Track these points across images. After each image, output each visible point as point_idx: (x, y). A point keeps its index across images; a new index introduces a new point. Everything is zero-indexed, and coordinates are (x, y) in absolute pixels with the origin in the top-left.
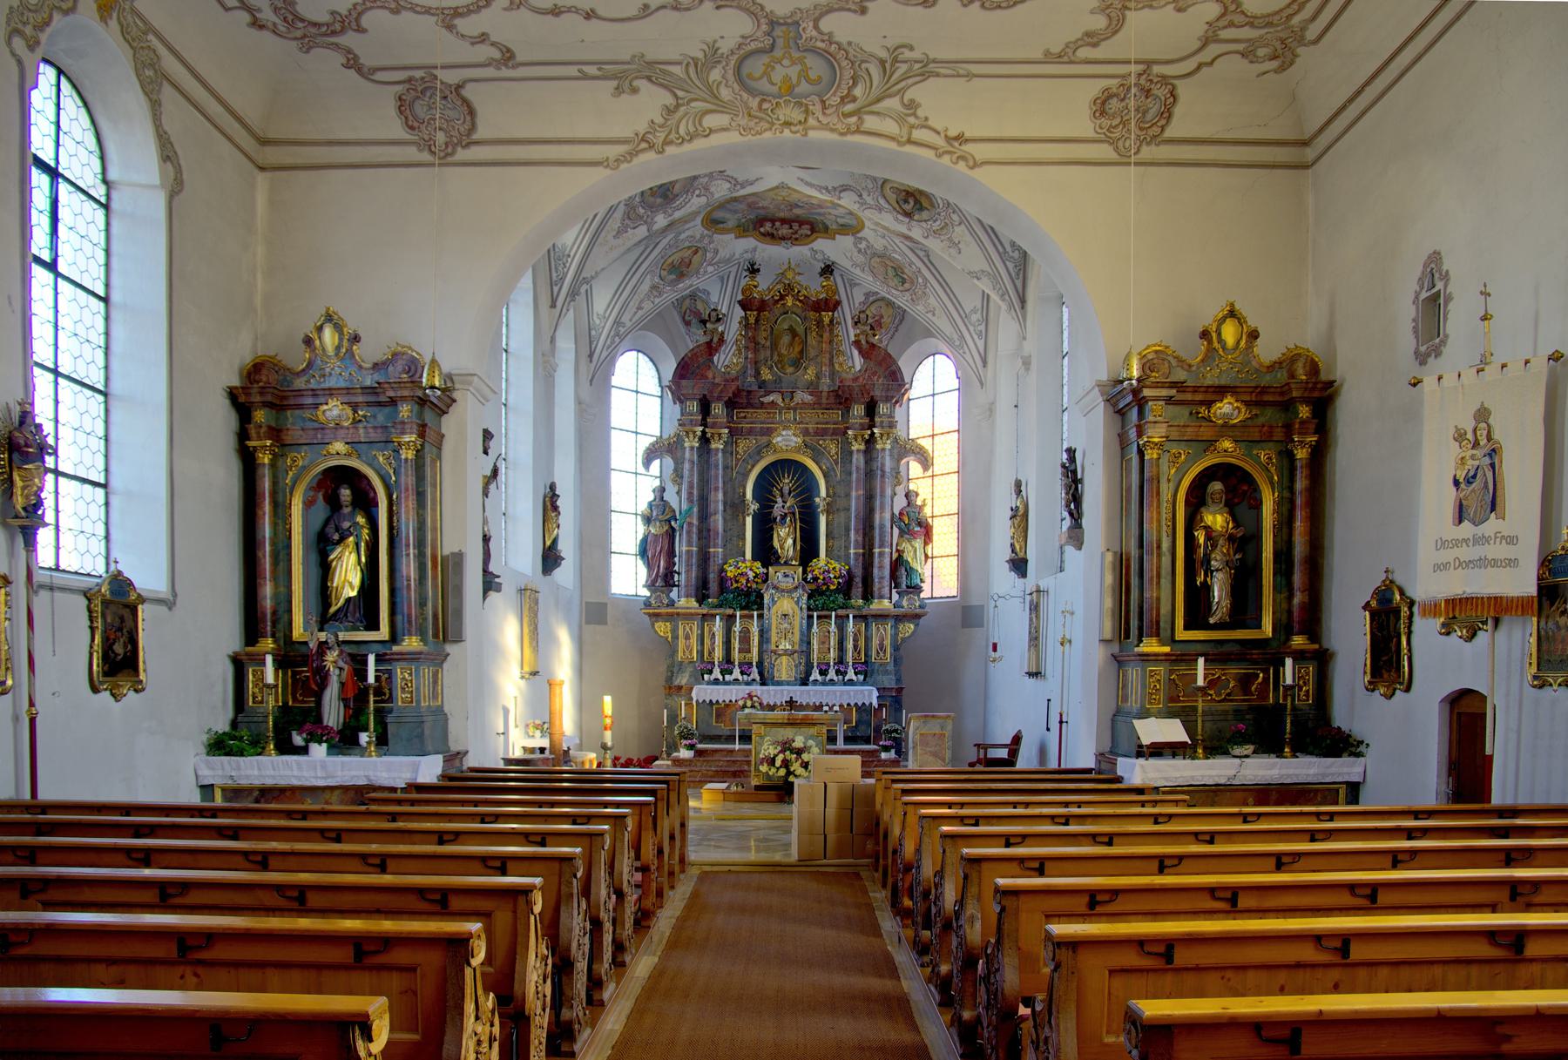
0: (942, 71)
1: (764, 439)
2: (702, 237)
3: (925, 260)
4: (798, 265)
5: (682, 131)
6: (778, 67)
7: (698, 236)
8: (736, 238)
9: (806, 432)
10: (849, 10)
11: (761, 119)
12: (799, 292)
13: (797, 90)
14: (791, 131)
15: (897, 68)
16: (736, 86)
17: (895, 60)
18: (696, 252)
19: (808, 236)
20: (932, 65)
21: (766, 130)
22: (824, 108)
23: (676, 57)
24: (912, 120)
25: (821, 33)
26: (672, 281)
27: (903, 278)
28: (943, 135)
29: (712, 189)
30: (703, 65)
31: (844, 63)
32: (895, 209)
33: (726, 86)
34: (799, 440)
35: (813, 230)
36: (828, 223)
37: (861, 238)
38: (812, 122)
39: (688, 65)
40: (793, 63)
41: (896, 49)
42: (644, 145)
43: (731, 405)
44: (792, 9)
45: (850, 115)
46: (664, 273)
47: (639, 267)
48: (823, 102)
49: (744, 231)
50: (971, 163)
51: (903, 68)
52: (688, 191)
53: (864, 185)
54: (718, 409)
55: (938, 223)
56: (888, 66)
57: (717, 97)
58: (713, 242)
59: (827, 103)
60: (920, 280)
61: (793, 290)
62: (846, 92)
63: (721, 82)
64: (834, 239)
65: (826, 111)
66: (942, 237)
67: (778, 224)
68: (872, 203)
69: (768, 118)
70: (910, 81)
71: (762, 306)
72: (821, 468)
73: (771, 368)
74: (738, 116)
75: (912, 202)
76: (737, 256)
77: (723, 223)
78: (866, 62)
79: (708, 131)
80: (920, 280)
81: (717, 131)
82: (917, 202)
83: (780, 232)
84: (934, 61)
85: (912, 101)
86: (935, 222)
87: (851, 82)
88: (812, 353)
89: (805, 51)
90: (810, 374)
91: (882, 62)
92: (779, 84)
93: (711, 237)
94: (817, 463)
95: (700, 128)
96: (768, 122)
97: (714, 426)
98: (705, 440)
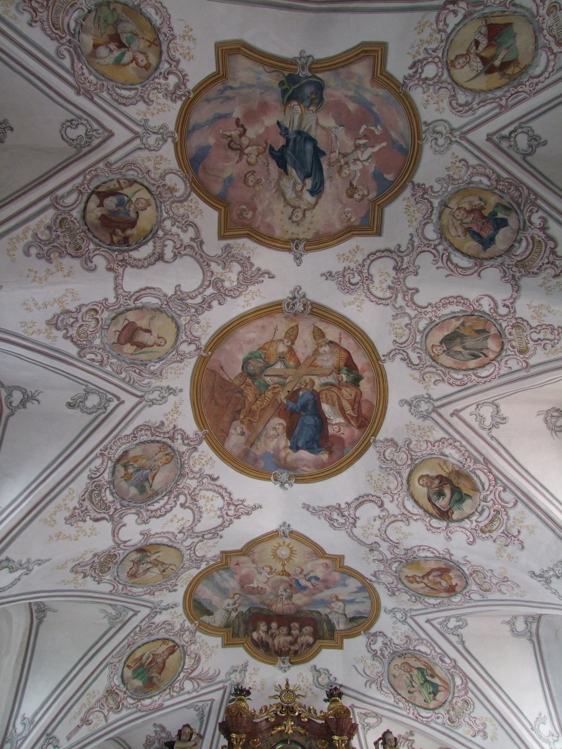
2: (183, 629)
3: (460, 647)
7: (178, 627)
8: (226, 645)
12: (300, 714)
18: (172, 651)
19: (309, 646)
26: (136, 690)
27: (435, 686)
29: (202, 502)
32: (426, 511)
35: (316, 636)
36: (334, 618)
37: (375, 635)
46: (128, 673)
52: (171, 492)
53: (385, 486)
55: (486, 513)
58: (194, 642)
60: (458, 681)
61: (293, 710)
64: (341, 647)
66: (494, 535)
67: (274, 625)
68: (397, 512)
75: (447, 491)
76: (222, 677)
80: (458, 681)
82: (455, 490)
83: (276, 641)
86: (481, 514)
93: (193, 633)
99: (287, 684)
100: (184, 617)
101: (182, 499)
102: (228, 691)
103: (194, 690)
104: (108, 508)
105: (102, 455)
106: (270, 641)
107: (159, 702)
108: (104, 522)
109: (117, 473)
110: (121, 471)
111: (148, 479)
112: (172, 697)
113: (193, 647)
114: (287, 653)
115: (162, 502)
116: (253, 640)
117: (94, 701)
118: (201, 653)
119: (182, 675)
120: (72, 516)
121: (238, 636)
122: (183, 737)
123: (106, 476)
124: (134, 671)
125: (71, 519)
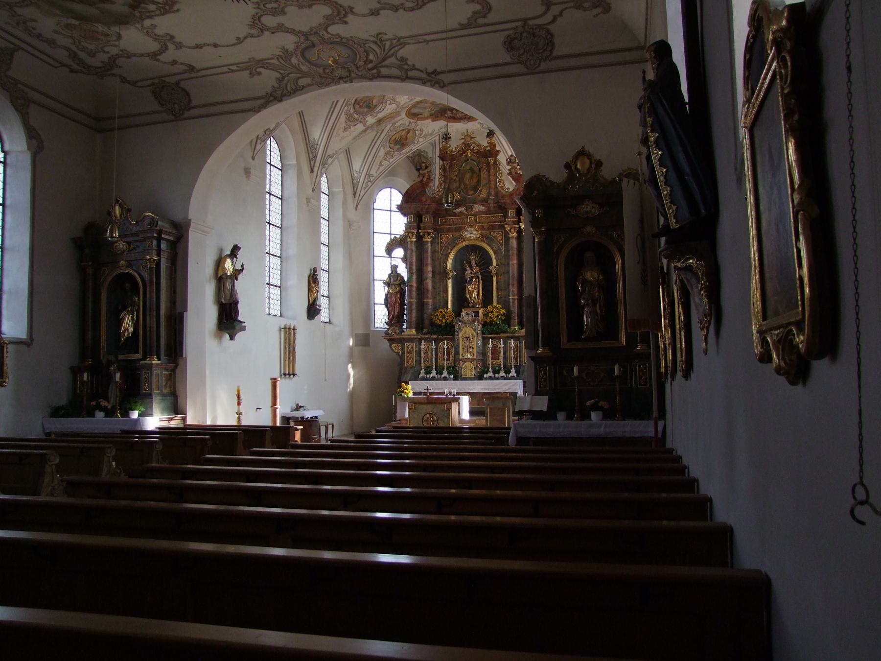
0: (409, 41)
1: (457, 234)
2: (410, 123)
4: (473, 133)
5: (289, 89)
9: (482, 228)
11: (327, 78)
12: (473, 148)
14: (344, 82)
15: (385, 44)
18: (409, 132)
20: (402, 40)
21: (331, 83)
22: (357, 68)
24: (406, 67)
26: (398, 149)
28: (425, 72)
30: (285, 57)
31: (356, 46)
34: (479, 233)
38: (353, 75)
42: (272, 98)
43: (436, 214)
45: (372, 69)
46: (392, 145)
47: (374, 145)
48: (356, 65)
49: (436, 118)
50: (442, 85)
51: (388, 44)
52: (382, 103)
54: (426, 218)
56: (379, 43)
57: (300, 71)
58: (418, 125)
59: (358, 65)
62: (365, 59)
65: (359, 69)
69: (330, 77)
70: (396, 48)
71: (453, 158)
72: (492, 249)
73: (459, 193)
74: (315, 78)
76: (436, 131)
77: (421, 114)
78: (366, 44)
79: (302, 87)
81: (306, 87)
83: (458, 116)
84: (402, 37)
85: (402, 58)
87: (365, 54)
88: (484, 182)
90: (484, 194)
93: (416, 122)
94: (490, 246)
95: (298, 86)
96: (331, 78)
97: (425, 228)
98: (420, 238)
99: (467, 132)
100: (409, 119)
101: (388, 102)
102: (441, 135)
103: (424, 140)
104: (357, 120)
105: (346, 105)
106: (455, 116)
107: (410, 148)
108: (358, 124)
109: (356, 108)
110: (357, 106)
111: (370, 104)
112: (415, 146)
113: (418, 127)
114: (465, 118)
115: (380, 107)
116: (446, 117)
117: (381, 159)
118: (423, 128)
119: (416, 138)
120: (345, 129)
121: (438, 117)
122: (423, 168)
123: (352, 110)
124: (394, 144)
125: (345, 130)
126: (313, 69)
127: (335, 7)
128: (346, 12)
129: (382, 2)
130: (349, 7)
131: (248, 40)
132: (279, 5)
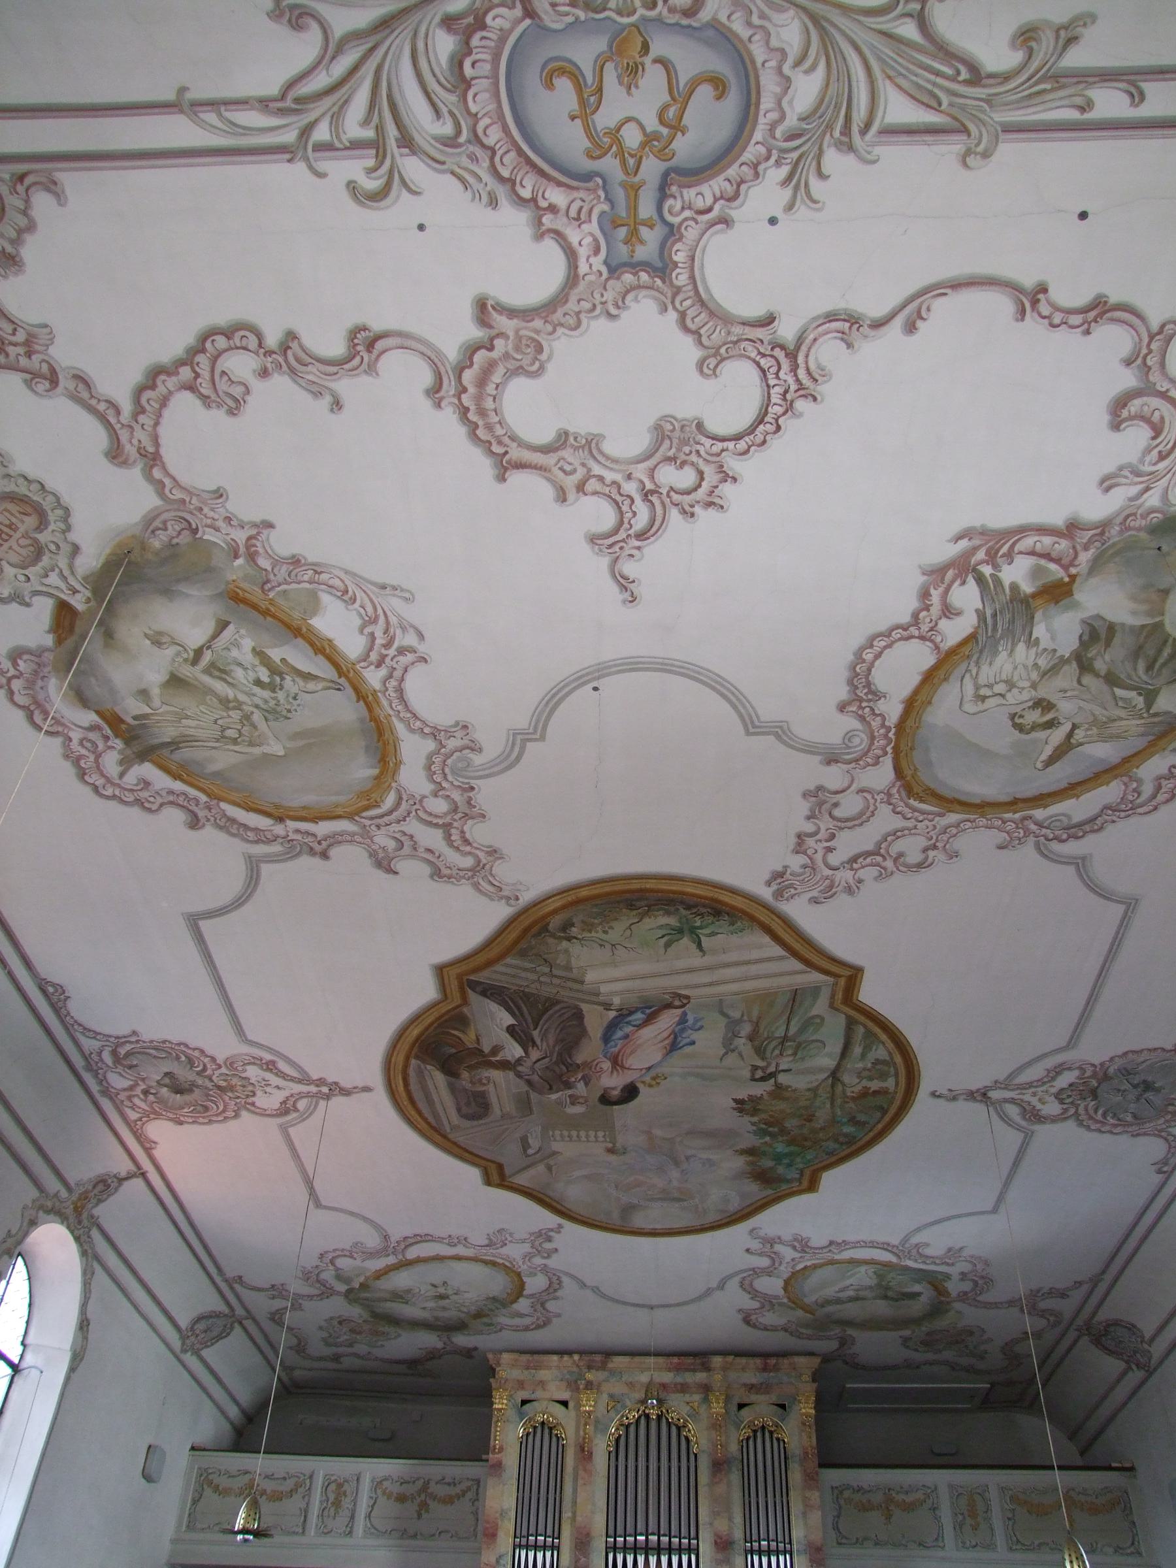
6: (652, 124)
10: (513, 313)
13: (600, 44)
15: (366, 122)
16: (758, 52)
17: (378, 146)
20: (289, 137)
23: (894, 154)
25: (559, 235)
30: (830, 127)
31: (494, 136)
33: (783, 117)
39: (868, 126)
40: (615, 133)
41: (388, 186)
44: (625, 315)
56: (392, 132)
62: (475, 41)
63: (798, 64)
70: (320, 81)
87: (468, 71)
89: (587, 177)
91: (407, 142)
92: (648, 60)
126: (749, 24)
127: (482, 413)
128: (459, 378)
129: (328, 399)
130: (438, 405)
131: (877, 311)
132: (651, 473)
